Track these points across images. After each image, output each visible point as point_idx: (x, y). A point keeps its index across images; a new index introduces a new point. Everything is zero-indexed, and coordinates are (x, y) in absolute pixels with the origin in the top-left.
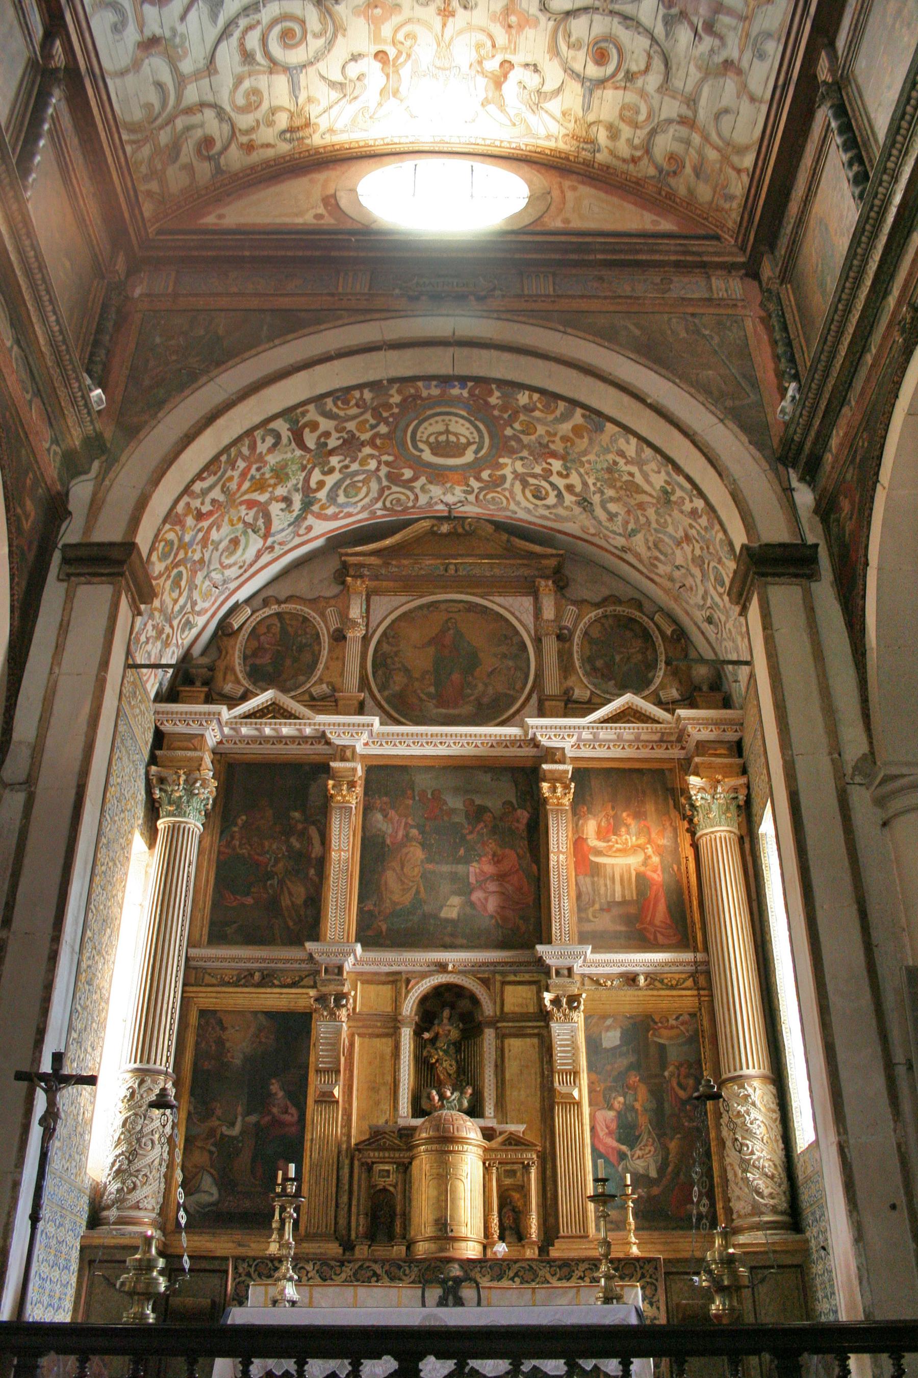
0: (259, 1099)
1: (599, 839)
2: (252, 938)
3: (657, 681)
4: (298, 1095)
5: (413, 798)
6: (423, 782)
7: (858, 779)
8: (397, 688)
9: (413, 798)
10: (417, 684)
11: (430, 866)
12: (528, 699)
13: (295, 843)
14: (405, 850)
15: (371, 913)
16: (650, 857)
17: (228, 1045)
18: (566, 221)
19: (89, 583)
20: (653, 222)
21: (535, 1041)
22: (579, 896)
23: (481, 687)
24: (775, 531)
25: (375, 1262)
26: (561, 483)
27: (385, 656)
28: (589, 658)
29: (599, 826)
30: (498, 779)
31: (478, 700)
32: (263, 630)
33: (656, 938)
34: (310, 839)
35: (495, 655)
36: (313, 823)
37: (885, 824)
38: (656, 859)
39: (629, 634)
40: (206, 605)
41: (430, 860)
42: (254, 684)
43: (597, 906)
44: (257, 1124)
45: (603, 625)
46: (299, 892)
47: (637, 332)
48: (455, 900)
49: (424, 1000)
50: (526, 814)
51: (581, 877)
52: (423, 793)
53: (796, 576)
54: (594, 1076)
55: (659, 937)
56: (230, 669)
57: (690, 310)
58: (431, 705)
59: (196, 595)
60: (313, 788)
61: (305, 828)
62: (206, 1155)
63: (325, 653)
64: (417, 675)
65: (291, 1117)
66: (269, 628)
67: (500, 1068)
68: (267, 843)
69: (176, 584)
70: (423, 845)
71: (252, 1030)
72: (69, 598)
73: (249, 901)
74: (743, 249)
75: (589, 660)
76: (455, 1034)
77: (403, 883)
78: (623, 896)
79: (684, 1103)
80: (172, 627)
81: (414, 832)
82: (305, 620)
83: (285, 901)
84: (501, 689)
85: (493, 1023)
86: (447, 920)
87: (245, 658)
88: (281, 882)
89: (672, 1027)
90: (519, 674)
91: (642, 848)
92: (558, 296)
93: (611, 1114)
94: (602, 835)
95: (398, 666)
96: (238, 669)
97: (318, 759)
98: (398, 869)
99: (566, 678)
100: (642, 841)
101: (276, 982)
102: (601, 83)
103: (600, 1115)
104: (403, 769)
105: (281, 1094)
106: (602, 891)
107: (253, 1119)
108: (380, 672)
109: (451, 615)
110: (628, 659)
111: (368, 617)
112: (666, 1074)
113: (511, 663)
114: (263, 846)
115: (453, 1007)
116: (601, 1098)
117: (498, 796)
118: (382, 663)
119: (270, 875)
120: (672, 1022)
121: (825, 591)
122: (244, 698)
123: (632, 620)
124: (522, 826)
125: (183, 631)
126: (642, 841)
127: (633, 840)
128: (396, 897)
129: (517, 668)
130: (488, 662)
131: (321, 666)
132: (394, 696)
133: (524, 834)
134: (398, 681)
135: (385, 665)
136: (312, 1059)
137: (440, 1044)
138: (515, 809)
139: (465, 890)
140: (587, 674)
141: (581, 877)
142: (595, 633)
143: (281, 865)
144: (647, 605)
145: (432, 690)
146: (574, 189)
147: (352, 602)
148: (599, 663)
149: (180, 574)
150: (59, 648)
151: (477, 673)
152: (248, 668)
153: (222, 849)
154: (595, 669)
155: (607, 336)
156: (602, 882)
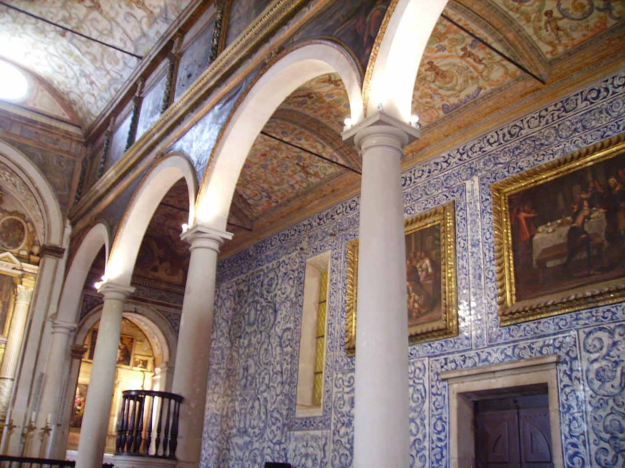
7: (51, 320)
18: (35, 105)
20: (64, 114)
24: (55, 241)
26: (8, 178)
37: (53, 333)
47: (41, 157)
57: (61, 154)
74: (85, 138)
92: (21, 136)
102: (59, 72)
121: (62, 262)
123: (20, 222)
144: (27, 217)
146: (42, 91)
155: (30, 156)
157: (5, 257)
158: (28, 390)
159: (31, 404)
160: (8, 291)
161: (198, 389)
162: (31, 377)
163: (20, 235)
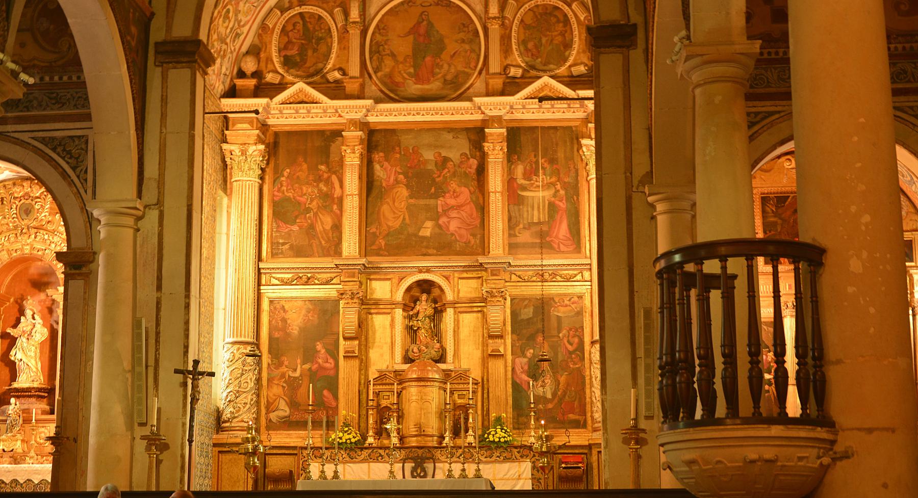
0: (309, 355)
1: (524, 179)
2: (299, 252)
3: (571, 60)
4: (333, 352)
5: (400, 153)
6: (408, 141)
8: (387, 70)
9: (400, 153)
10: (401, 66)
11: (412, 201)
12: (480, 73)
13: (322, 185)
14: (395, 191)
15: (374, 233)
16: (558, 191)
17: (289, 322)
19: (175, 68)
21: (479, 315)
22: (510, 219)
23: (446, 66)
25: (381, 448)
27: (378, 44)
28: (523, 41)
29: (525, 169)
30: (457, 137)
31: (444, 76)
32: (290, 27)
33: (559, 248)
34: (333, 187)
35: (456, 41)
36: (335, 173)
38: (562, 192)
39: (553, 20)
40: (248, 18)
41: (411, 197)
42: (287, 72)
43: (521, 226)
44: (310, 369)
45: (534, 12)
46: (327, 221)
48: (429, 224)
49: (409, 289)
50: (476, 162)
51: (511, 206)
52: (406, 149)
53: (620, 47)
54: (515, 337)
55: (561, 246)
56: (269, 60)
58: (410, 82)
59: (240, 17)
60: (333, 147)
61: (329, 177)
62: (281, 389)
63: (335, 45)
64: (401, 59)
65: (330, 364)
66: (294, 25)
67: (456, 332)
68: (304, 188)
69: (227, 17)
70: (408, 186)
71: (304, 312)
72: (164, 78)
73: (295, 228)
75: (523, 43)
76: (430, 311)
77: (394, 213)
78: (539, 219)
79: (570, 353)
80: (227, 44)
81: (401, 177)
82: (320, 17)
83: (319, 228)
84: (460, 67)
85: (453, 304)
86: (424, 237)
87: (280, 51)
88: (316, 214)
89: (566, 306)
90: (473, 55)
91: (554, 184)
93: (525, 360)
94: (527, 176)
95: (388, 52)
96: (275, 60)
97: (334, 127)
98: (391, 203)
99: (506, 58)
100: (553, 180)
101: (317, 282)
103: (517, 360)
104: (393, 132)
105: (323, 351)
106: (525, 216)
107: (307, 366)
108: (375, 58)
109: (424, 9)
110: (552, 41)
111: (364, 15)
112: (561, 335)
113: (467, 47)
114: (302, 190)
115: (428, 292)
116: (519, 351)
117: (456, 150)
118: (377, 49)
119: (308, 210)
120: (567, 302)
122: (281, 87)
124: (473, 171)
125: (234, 41)
126: (553, 180)
127: (548, 179)
128: (390, 224)
129: (472, 51)
130: (452, 47)
131: (333, 56)
132: (385, 76)
133: (475, 177)
134: (388, 63)
135: (378, 52)
136: (341, 329)
137: (421, 316)
138: (468, 159)
139: (436, 218)
140: (521, 54)
141: (511, 206)
142: (528, 21)
143: (314, 203)
145: (412, 70)
147: (352, 5)
148: (530, 45)
149: (229, 10)
150: (163, 116)
151: (443, 56)
152: (282, 59)
153: (276, 193)
154: (527, 50)
156: (525, 209)
157: (542, 89)
158: (627, 350)
159: (641, 381)
160: (570, 159)
161: (866, 218)
162: (626, 322)
163: (563, 34)
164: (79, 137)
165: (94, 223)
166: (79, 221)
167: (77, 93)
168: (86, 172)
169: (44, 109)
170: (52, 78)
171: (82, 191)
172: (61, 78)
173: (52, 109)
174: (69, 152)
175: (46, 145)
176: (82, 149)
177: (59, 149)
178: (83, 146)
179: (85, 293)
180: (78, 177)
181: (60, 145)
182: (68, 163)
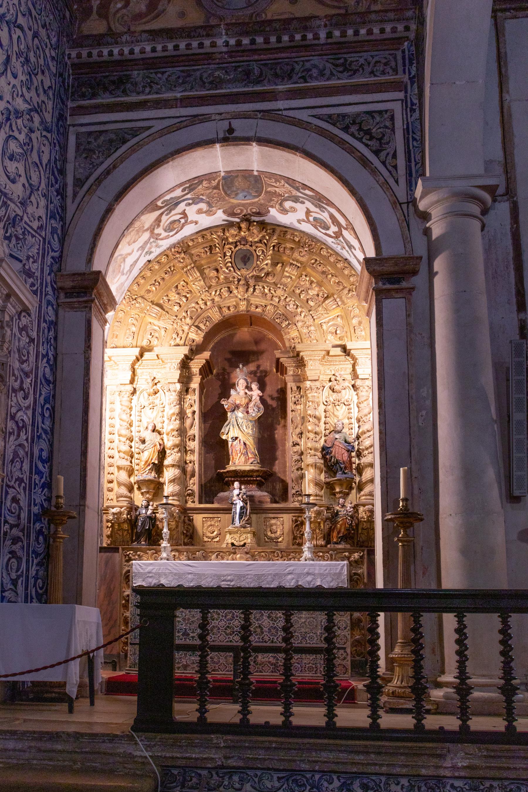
164: (380, 112)
165: (414, 221)
166: (390, 220)
167: (372, 57)
168: (395, 156)
169: (328, 79)
170: (344, 34)
171: (391, 181)
172: (356, 33)
173: (339, 79)
174: (368, 132)
175: (334, 125)
176: (386, 127)
177: (353, 129)
178: (388, 124)
179: (408, 316)
180: (384, 163)
181: (354, 123)
182: (367, 145)
